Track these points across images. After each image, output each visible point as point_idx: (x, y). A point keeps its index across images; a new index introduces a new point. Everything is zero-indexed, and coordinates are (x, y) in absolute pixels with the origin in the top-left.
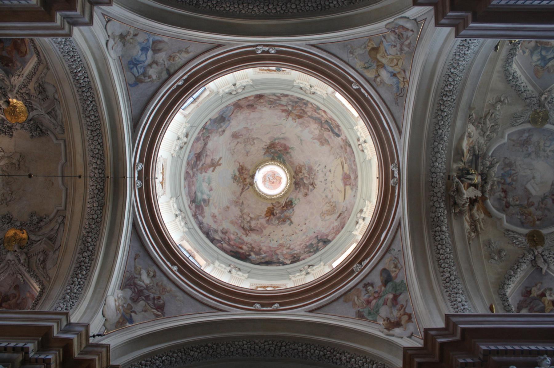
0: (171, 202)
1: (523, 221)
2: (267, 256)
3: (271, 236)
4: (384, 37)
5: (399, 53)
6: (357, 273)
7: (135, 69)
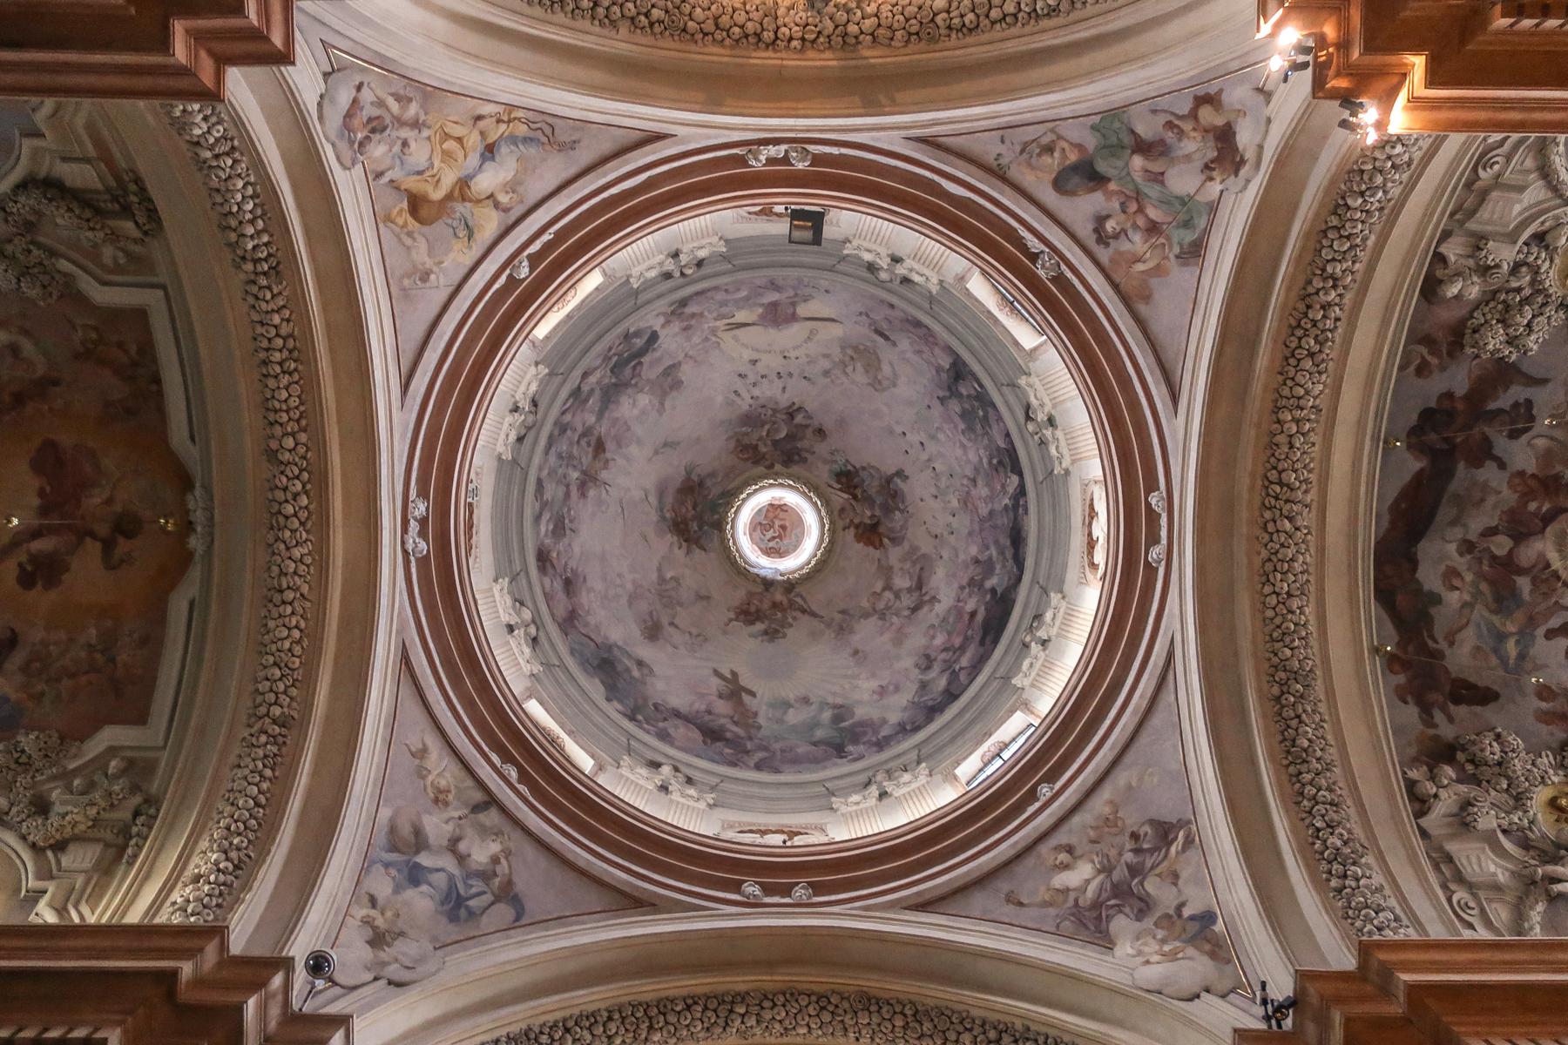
0: (844, 809)
2: (996, 542)
3: (938, 532)
4: (379, 175)
5: (426, 133)
6: (1063, 267)
7: (471, 903)
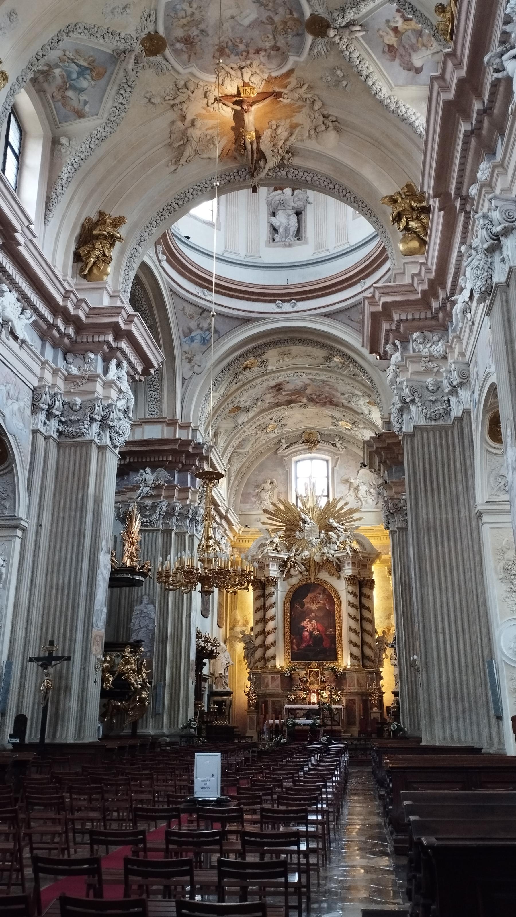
1: (294, 32)
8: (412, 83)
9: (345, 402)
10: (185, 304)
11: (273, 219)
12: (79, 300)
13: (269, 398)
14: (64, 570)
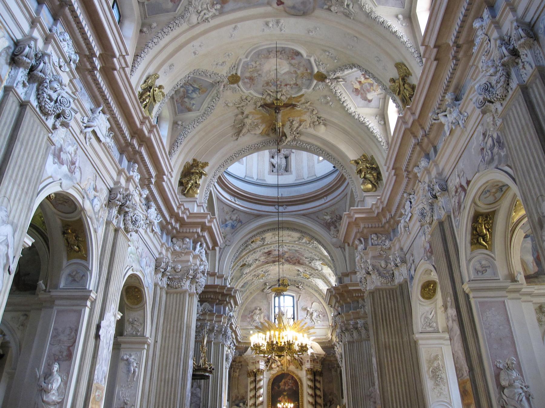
8: (367, 106)
9: (307, 263)
10: (224, 206)
11: (272, 160)
12: (185, 209)
13: (263, 259)
14: (169, 370)
